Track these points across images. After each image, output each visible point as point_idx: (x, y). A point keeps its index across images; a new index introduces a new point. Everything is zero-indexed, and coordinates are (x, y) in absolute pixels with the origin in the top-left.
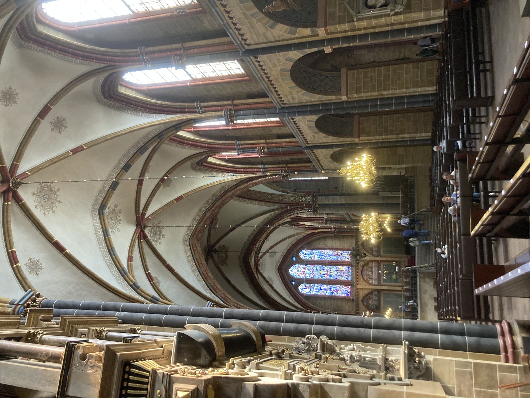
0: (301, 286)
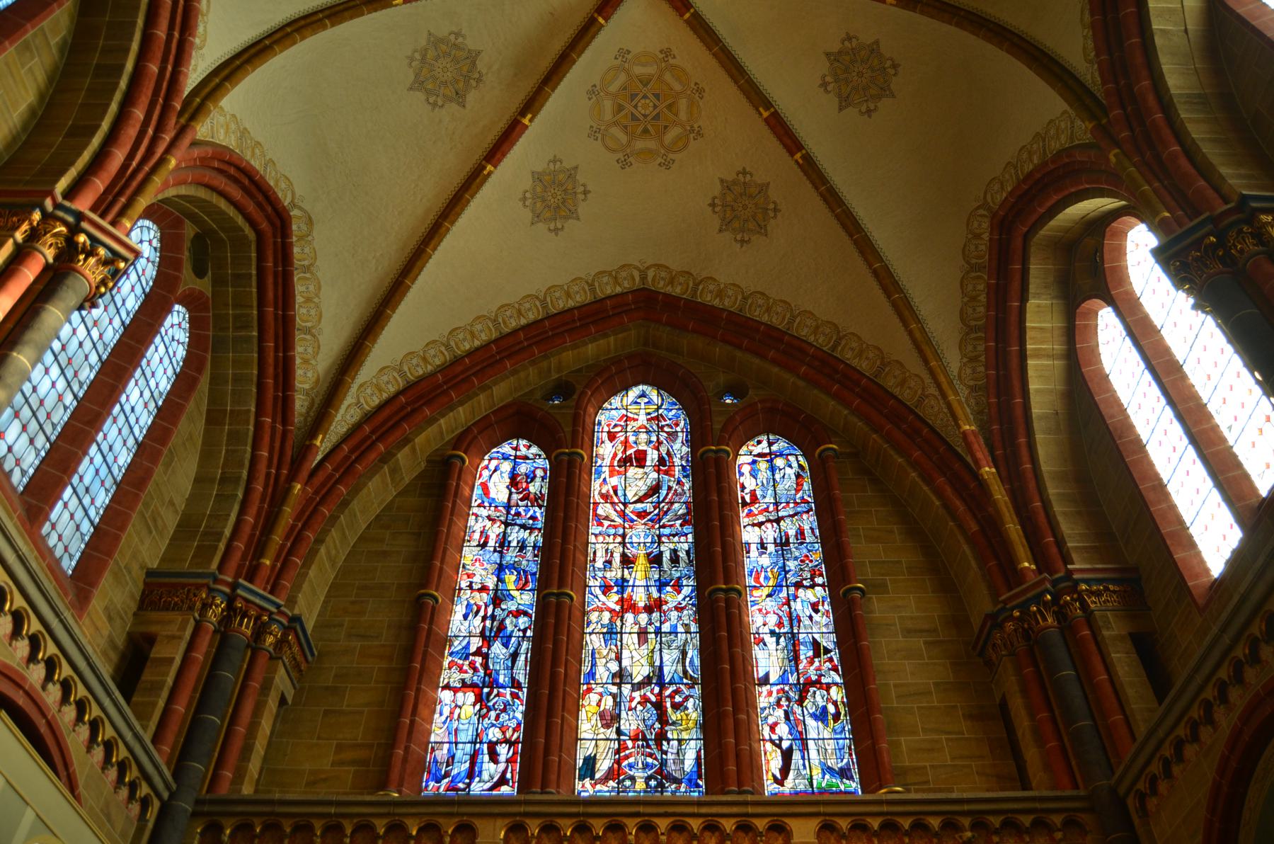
0: (534, 450)
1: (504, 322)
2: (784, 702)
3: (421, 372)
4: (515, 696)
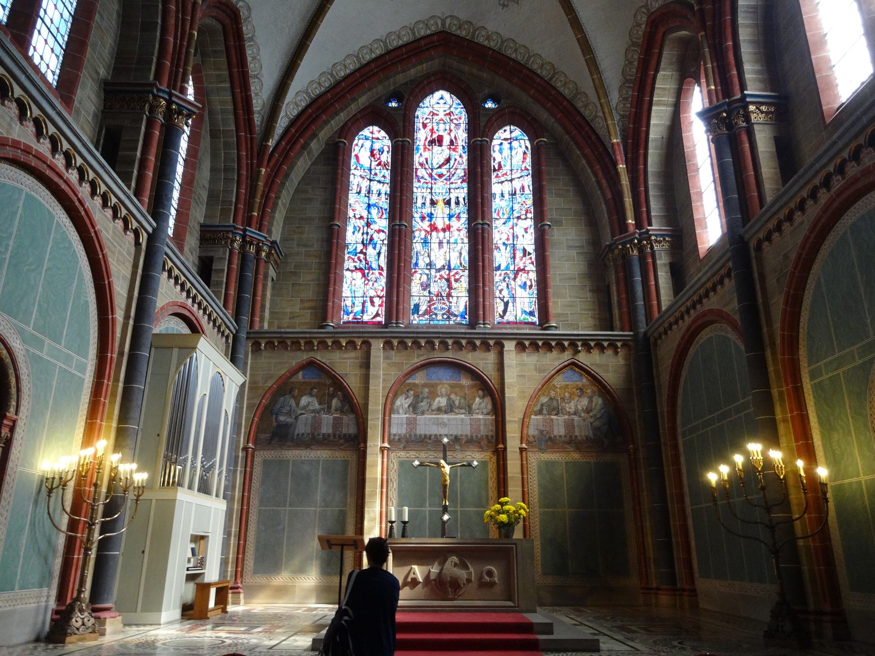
0: (383, 133)
1: (363, 58)
2: (507, 279)
3: (318, 92)
4: (380, 274)
